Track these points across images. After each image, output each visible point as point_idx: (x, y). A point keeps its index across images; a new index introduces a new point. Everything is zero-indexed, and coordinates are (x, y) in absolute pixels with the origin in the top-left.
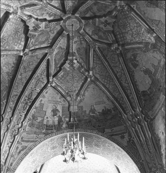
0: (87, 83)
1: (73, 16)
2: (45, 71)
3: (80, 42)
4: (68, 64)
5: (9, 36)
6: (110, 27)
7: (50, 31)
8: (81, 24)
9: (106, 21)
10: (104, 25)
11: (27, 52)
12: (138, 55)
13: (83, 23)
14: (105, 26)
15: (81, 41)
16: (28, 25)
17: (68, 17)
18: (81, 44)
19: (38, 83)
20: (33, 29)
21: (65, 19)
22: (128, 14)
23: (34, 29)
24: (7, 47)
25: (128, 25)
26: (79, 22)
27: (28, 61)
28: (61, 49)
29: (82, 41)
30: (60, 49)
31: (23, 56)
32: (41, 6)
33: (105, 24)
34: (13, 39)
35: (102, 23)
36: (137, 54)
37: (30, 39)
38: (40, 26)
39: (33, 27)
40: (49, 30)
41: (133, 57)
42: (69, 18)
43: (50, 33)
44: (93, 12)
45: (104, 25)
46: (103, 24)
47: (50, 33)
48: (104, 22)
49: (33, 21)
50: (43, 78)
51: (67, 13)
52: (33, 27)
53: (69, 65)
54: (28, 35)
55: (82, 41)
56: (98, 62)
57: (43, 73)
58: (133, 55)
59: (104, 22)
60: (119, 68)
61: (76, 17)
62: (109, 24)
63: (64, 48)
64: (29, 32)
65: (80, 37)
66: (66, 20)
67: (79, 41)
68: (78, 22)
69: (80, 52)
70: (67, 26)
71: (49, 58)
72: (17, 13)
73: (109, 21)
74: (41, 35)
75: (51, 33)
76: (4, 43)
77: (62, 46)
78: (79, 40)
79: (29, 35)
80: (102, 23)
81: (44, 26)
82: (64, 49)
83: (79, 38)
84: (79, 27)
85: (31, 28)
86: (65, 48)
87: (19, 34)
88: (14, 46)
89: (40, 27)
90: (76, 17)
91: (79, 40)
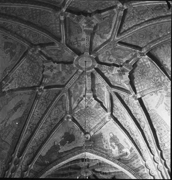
0: (66, 6)
1: (84, 70)
2: (128, 19)
3: (78, 40)
4: (94, 22)
5: (149, 79)
6: (47, 65)
7: (110, 55)
8: (76, 64)
9: (52, 71)
10: (53, 67)
11: (140, 56)
12: (9, 59)
13: (75, 65)
14: (52, 66)
15: (77, 41)
16: (128, 79)
17: (90, 70)
18: (76, 39)
19: (141, 11)
20: (126, 73)
21: (92, 68)
22: (33, 83)
23: (124, 71)
24: (157, 71)
25: (29, 74)
26: (78, 65)
27: (144, 40)
28: (100, 35)
29: (75, 42)
30: (102, 35)
31: (145, 54)
32: (112, 90)
33: (52, 68)
34: (148, 72)
35: (55, 68)
36: (11, 59)
37: (132, 65)
38: (118, 72)
39: (125, 74)
40: (111, 56)
41: (14, 51)
42: (89, 69)
43: (111, 53)
44: (66, 70)
45: (53, 67)
46: (55, 67)
47: (111, 53)
48: (54, 69)
49: (123, 80)
50: (133, 13)
51: (90, 74)
52: (125, 74)
53: (92, 22)
54: (132, 68)
55: (75, 42)
56: (54, 25)
57: (130, 17)
58: (15, 53)
59: (54, 69)
60: (25, 33)
61: (81, 69)
62: (49, 68)
63: (97, 34)
64: (130, 71)
65: (78, 46)
66: (92, 68)
67: (79, 41)
68: (80, 65)
69: (78, 30)
70: (92, 61)
71: (117, 38)
72: (133, 96)
73: (49, 71)
74: (120, 57)
75: (109, 53)
76: (157, 78)
77: (99, 37)
78: (78, 42)
79: (132, 68)
80: (55, 68)
81: (114, 70)
82: (97, 33)
83: (79, 44)
84: (79, 61)
85: (127, 74)
86: (96, 34)
87: (142, 69)
88: (151, 66)
89: (118, 71)
90: (81, 69)
91: (78, 42)
